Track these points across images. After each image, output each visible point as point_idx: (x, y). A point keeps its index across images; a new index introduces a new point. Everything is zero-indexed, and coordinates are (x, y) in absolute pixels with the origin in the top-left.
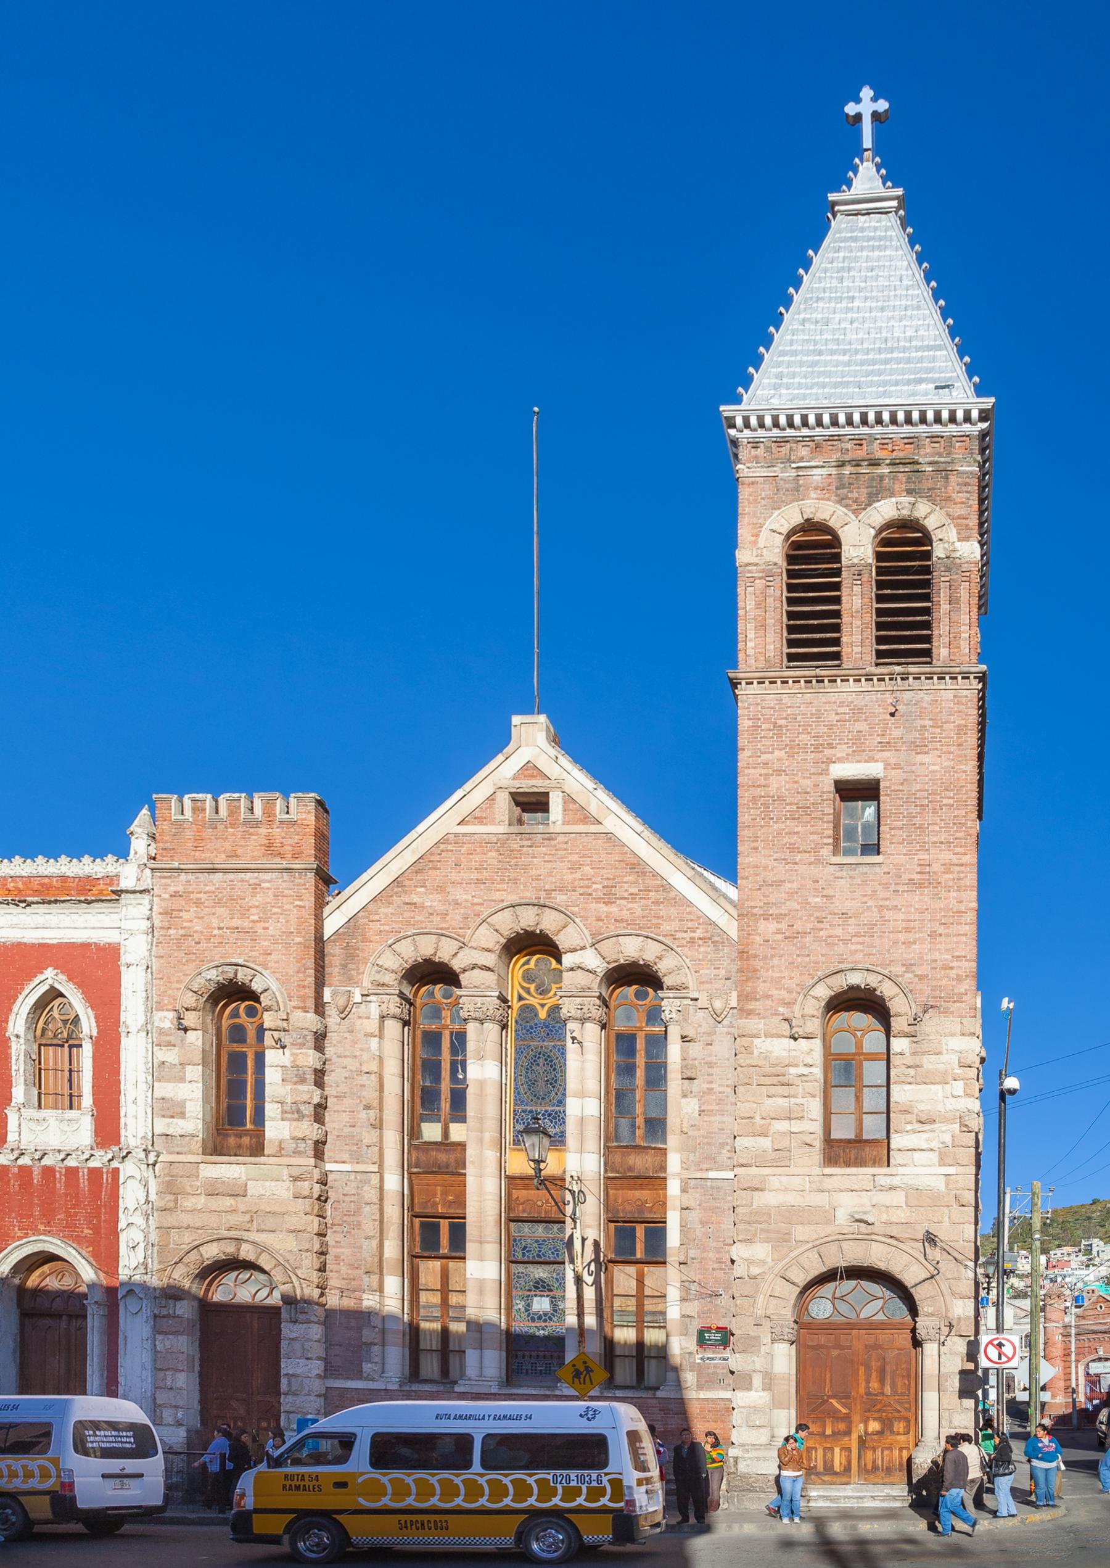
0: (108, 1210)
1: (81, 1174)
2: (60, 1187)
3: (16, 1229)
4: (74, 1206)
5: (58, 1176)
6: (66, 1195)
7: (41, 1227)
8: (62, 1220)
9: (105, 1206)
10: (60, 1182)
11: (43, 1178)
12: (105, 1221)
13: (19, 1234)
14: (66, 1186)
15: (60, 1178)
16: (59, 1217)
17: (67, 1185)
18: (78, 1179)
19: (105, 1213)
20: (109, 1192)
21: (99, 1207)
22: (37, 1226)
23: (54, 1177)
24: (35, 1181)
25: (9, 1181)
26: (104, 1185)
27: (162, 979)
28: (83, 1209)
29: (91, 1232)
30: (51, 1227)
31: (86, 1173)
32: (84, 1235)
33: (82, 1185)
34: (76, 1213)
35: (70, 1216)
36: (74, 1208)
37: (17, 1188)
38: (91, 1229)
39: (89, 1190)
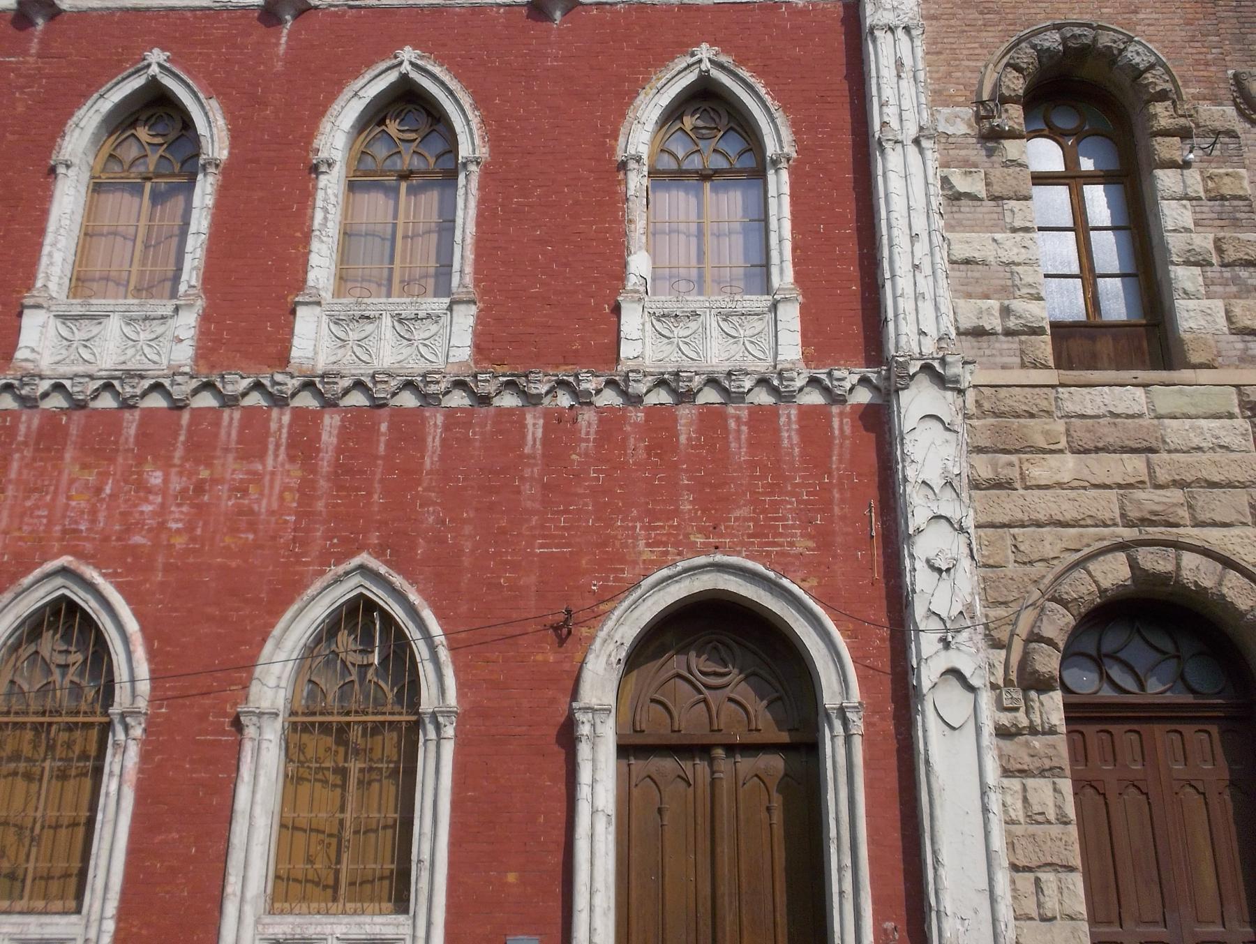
0: (848, 495)
1: (783, 420)
2: (739, 449)
3: (642, 543)
4: (772, 489)
5: (732, 424)
6: (752, 465)
7: (699, 539)
8: (746, 519)
9: (841, 484)
10: (738, 439)
11: (700, 432)
12: (843, 518)
13: (647, 554)
14: (750, 445)
15: (738, 431)
16: (738, 513)
17: (753, 445)
18: (777, 431)
19: (842, 500)
20: (847, 456)
21: (827, 489)
22: (687, 536)
23: (725, 428)
24: (683, 439)
25: (624, 440)
26: (837, 442)
27: (939, 53)
28: (792, 494)
29: (811, 544)
30: (721, 536)
31: (793, 418)
32: (795, 551)
33: (786, 443)
34: (775, 506)
35: (764, 511)
36: (772, 493)
37: (642, 454)
38: (810, 537)
39: (802, 455)
